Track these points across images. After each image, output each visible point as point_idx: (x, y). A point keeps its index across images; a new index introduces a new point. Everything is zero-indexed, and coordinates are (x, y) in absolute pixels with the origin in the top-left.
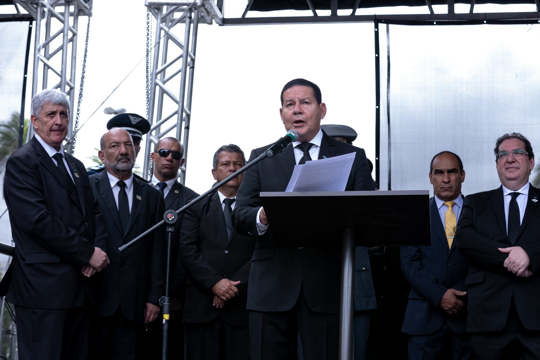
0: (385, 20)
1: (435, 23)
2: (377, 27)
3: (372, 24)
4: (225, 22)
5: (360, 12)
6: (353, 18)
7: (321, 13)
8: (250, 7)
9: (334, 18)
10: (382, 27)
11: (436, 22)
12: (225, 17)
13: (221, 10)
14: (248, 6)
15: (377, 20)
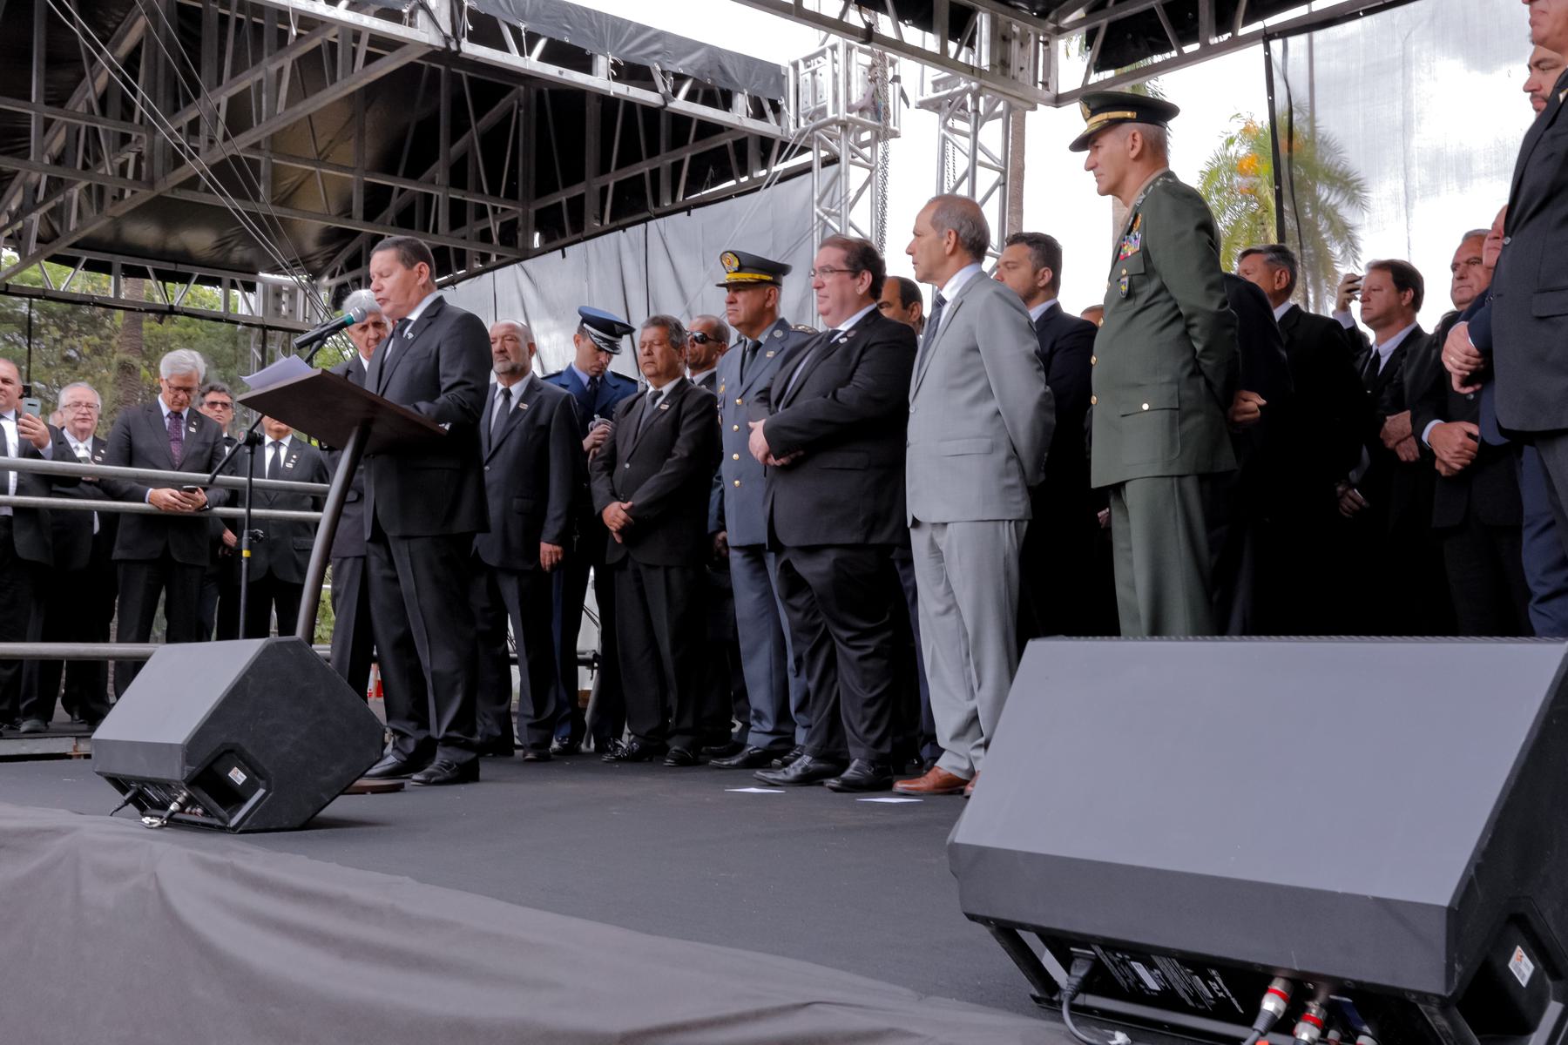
0: (1279, 33)
1: (1361, 14)
2: (1267, 48)
3: (1260, 47)
4: (1059, 100)
5: (1243, 31)
6: (1237, 43)
7: (1189, 49)
8: (1096, 65)
9: (1208, 52)
10: (1276, 45)
11: (1363, 11)
12: (1060, 92)
13: (1045, 84)
14: (1088, 67)
15: (1267, 36)
